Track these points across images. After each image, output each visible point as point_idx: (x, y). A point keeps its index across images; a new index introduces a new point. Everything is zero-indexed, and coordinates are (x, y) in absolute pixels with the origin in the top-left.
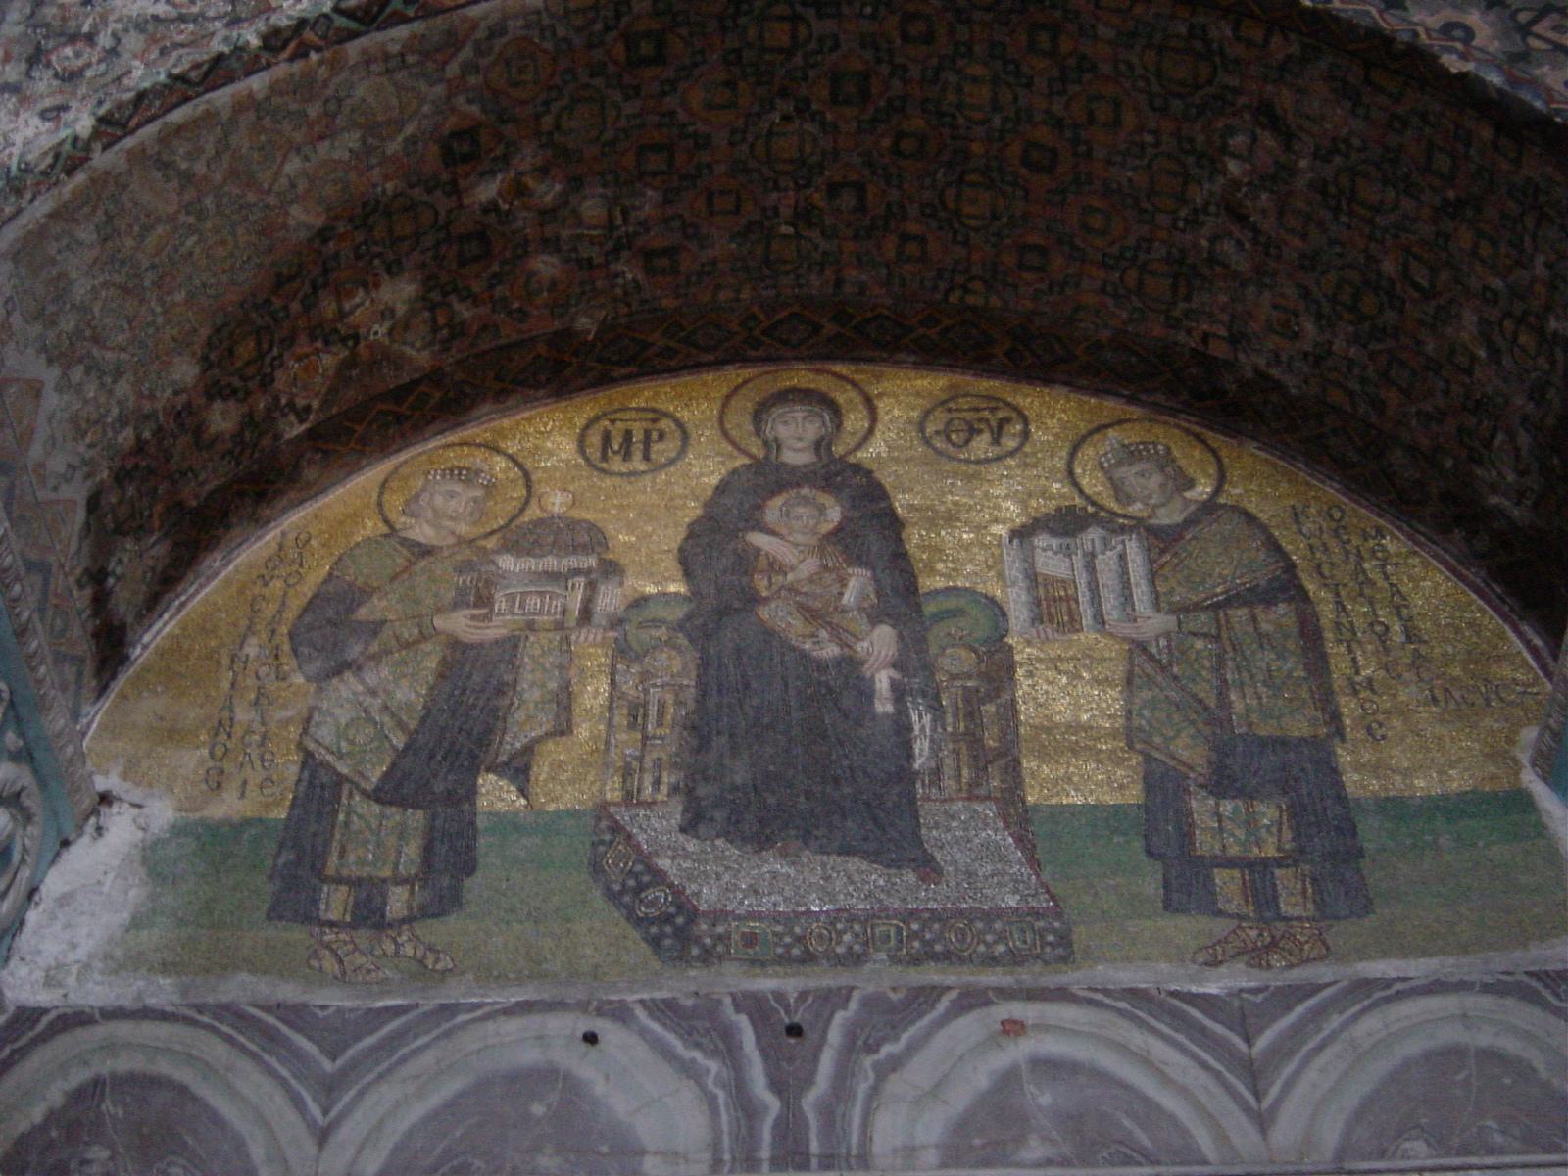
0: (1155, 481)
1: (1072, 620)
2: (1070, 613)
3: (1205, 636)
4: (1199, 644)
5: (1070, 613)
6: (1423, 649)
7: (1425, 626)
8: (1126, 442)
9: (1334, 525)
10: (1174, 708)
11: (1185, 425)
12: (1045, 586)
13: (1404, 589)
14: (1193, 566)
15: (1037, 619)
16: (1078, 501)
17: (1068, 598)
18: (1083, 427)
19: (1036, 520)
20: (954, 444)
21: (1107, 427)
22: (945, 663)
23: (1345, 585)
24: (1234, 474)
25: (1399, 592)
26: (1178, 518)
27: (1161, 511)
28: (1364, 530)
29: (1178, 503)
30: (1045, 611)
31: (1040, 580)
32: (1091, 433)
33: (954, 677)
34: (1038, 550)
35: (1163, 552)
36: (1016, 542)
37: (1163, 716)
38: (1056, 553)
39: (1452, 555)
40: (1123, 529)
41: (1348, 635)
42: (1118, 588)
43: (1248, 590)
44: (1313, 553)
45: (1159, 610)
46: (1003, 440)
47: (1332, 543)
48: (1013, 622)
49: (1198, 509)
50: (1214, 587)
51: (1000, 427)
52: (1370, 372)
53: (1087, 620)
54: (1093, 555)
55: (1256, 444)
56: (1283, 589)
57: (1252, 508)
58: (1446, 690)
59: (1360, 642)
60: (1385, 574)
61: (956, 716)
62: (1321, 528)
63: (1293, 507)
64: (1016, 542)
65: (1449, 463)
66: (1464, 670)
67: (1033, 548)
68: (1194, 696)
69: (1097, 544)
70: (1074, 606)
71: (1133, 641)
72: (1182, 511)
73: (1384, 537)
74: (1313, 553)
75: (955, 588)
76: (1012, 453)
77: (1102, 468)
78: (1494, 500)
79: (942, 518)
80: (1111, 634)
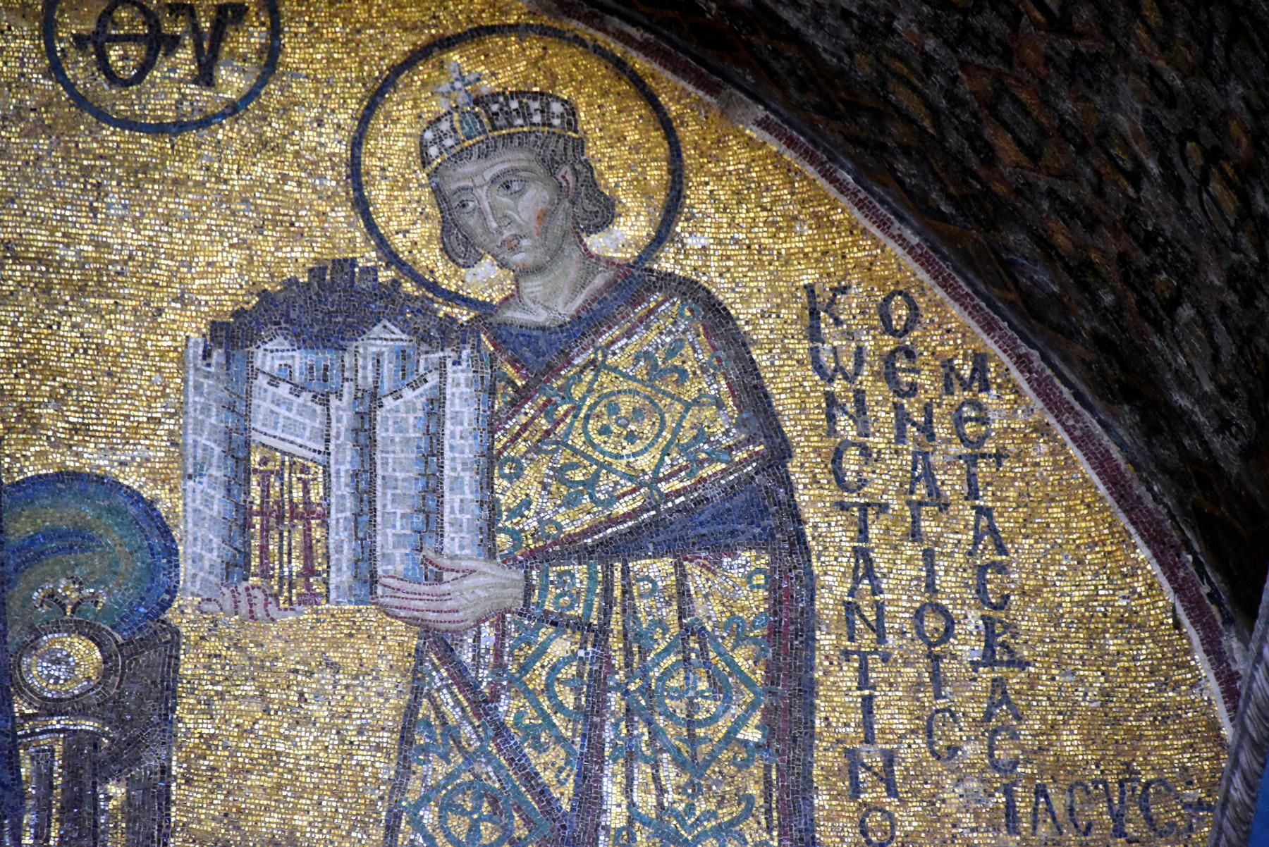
0: (536, 196)
1: (309, 571)
2: (308, 548)
3: (581, 625)
4: (561, 647)
5: (308, 548)
6: (1016, 680)
7: (1029, 621)
8: (487, 86)
9: (889, 343)
10: (486, 808)
11: (618, 49)
12: (265, 476)
13: (999, 523)
14: (579, 442)
15: (236, 566)
16: (368, 256)
17: (306, 513)
18: (402, 45)
19: (264, 294)
20: (112, 77)
21: (447, 43)
22: (37, 672)
23: (883, 508)
24: (697, 195)
25: (993, 531)
26: (565, 308)
27: (532, 287)
28: (948, 364)
29: (571, 266)
30: (255, 543)
31: (256, 458)
32: (410, 62)
33: (52, 707)
34: (262, 381)
35: (522, 396)
36: (217, 355)
37: (459, 826)
38: (297, 390)
39: (1121, 445)
40: (447, 334)
41: (867, 640)
42: (415, 489)
43: (678, 510)
44: (831, 418)
45: (491, 554)
46: (222, 73)
47: (877, 393)
48: (185, 569)
49: (610, 285)
50: (614, 499)
51: (218, 35)
52: (965, 89)
53: (341, 576)
54: (375, 397)
55: (760, 112)
56: (754, 513)
57: (727, 298)
58: (1041, 791)
59: (885, 658)
60: (971, 480)
61: (44, 807)
62: (860, 350)
63: (810, 289)
64: (217, 355)
65: (1108, 299)
66: (1088, 740)
67: (256, 373)
68: (530, 777)
69: (387, 368)
70: (317, 534)
71: (426, 630)
72: (575, 292)
73: (985, 387)
74: (831, 418)
75: (76, 475)
76: (233, 110)
77: (425, 162)
78: (1182, 400)
79: (67, 283)
80: (385, 610)
